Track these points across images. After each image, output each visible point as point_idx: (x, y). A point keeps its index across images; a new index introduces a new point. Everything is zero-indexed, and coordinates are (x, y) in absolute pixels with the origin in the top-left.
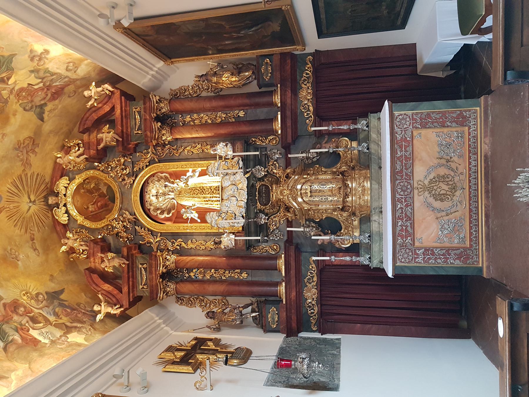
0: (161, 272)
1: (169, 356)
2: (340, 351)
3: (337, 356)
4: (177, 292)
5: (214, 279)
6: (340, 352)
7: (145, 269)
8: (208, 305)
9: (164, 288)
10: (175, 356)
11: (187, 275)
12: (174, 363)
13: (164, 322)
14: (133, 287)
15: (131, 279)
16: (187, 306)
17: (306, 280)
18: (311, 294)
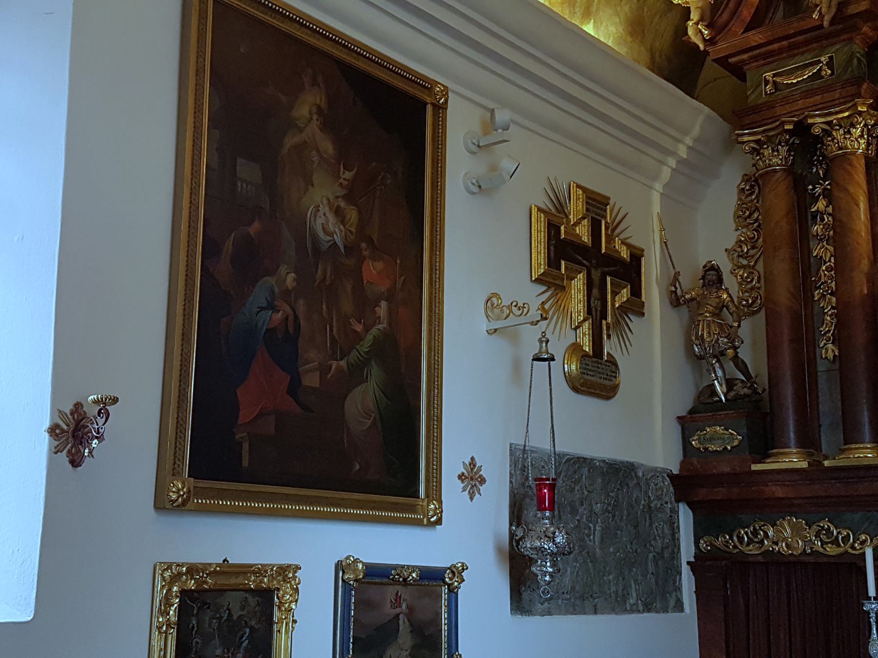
0: (810, 121)
1: (576, 208)
2: (639, 611)
3: (619, 604)
4: (769, 174)
5: (813, 269)
6: (632, 611)
7: (818, 75)
8: (745, 262)
9: (769, 139)
10: (576, 224)
11: (818, 190)
12: (552, 228)
13: (681, 161)
14: (767, 56)
15: (785, 43)
16: (739, 207)
17: (825, 524)
18: (787, 537)
